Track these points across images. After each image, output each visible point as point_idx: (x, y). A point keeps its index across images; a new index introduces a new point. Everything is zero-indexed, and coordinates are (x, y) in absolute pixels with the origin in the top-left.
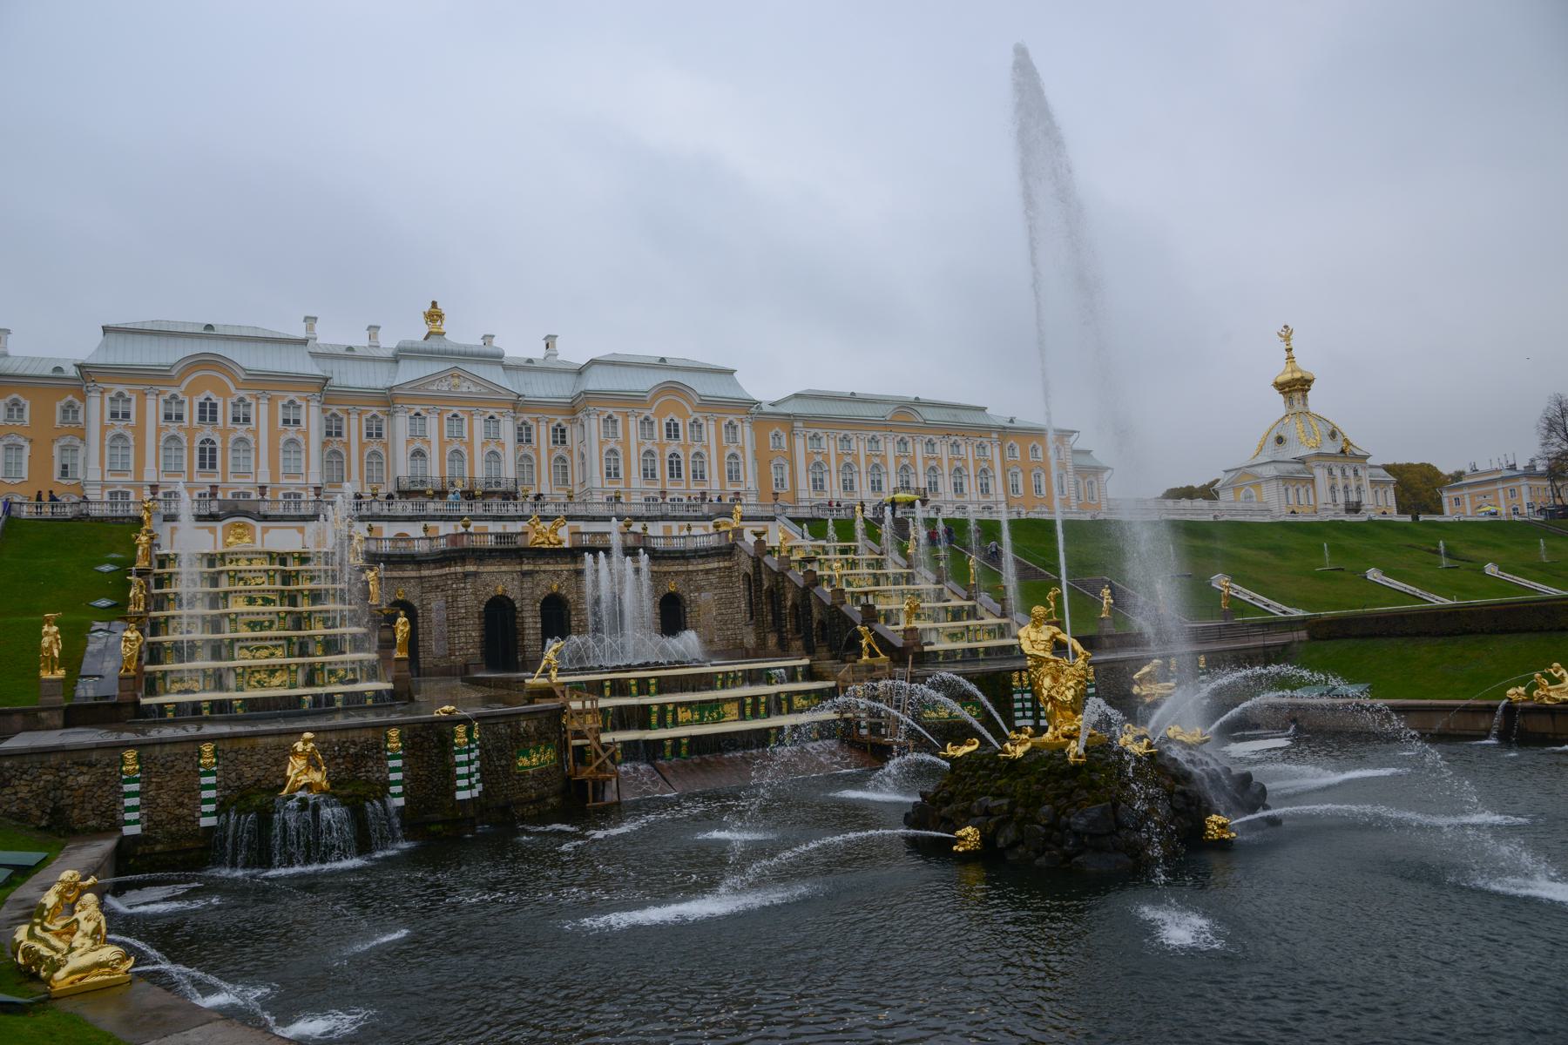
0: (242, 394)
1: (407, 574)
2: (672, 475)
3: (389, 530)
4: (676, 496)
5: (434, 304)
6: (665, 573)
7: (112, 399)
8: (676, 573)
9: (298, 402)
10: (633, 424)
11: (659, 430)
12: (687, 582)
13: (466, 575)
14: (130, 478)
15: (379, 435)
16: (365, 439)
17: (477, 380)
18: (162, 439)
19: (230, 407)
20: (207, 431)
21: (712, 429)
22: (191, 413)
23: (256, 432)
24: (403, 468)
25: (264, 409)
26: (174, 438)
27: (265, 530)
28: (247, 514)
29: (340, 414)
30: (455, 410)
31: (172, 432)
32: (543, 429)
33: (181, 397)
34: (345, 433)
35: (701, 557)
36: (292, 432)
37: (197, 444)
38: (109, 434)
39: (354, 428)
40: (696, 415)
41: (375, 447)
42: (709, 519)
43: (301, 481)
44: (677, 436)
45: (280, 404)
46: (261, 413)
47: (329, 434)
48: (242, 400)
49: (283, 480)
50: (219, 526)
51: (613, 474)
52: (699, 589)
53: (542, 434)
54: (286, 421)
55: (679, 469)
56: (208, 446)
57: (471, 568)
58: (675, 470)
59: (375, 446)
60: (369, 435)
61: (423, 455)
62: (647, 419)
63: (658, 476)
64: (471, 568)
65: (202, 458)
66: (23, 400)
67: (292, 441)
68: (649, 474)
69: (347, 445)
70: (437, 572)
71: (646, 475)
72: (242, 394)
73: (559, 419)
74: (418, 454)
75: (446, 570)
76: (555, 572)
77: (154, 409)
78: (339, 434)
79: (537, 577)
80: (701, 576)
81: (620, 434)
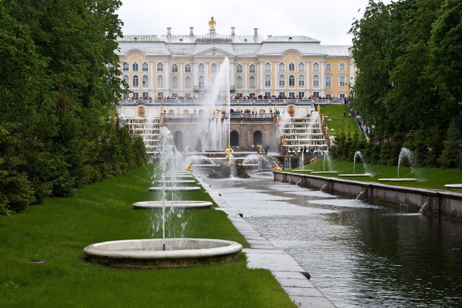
1: (180, 124)
2: (290, 84)
4: (292, 92)
5: (212, 18)
8: (259, 125)
10: (276, 66)
11: (287, 67)
12: (262, 127)
13: (194, 125)
15: (190, 71)
17: (221, 51)
19: (142, 64)
20: (136, 73)
22: (131, 67)
23: (150, 73)
27: (148, 109)
28: (143, 104)
29: (177, 64)
30: (214, 62)
36: (160, 73)
37: (132, 77)
39: (181, 69)
41: (188, 75)
42: (286, 105)
43: (163, 89)
44: (293, 69)
47: (173, 71)
49: (158, 89)
50: (136, 107)
51: (268, 84)
52: (266, 130)
53: (246, 69)
54: (158, 69)
55: (293, 82)
56: (136, 78)
57: (195, 123)
58: (292, 83)
59: (188, 74)
60: (186, 71)
62: (282, 63)
63: (285, 84)
64: (195, 123)
65: (134, 82)
67: (160, 76)
68: (282, 83)
71: (280, 84)
72: (145, 61)
78: (177, 71)
80: (266, 126)
81: (271, 70)
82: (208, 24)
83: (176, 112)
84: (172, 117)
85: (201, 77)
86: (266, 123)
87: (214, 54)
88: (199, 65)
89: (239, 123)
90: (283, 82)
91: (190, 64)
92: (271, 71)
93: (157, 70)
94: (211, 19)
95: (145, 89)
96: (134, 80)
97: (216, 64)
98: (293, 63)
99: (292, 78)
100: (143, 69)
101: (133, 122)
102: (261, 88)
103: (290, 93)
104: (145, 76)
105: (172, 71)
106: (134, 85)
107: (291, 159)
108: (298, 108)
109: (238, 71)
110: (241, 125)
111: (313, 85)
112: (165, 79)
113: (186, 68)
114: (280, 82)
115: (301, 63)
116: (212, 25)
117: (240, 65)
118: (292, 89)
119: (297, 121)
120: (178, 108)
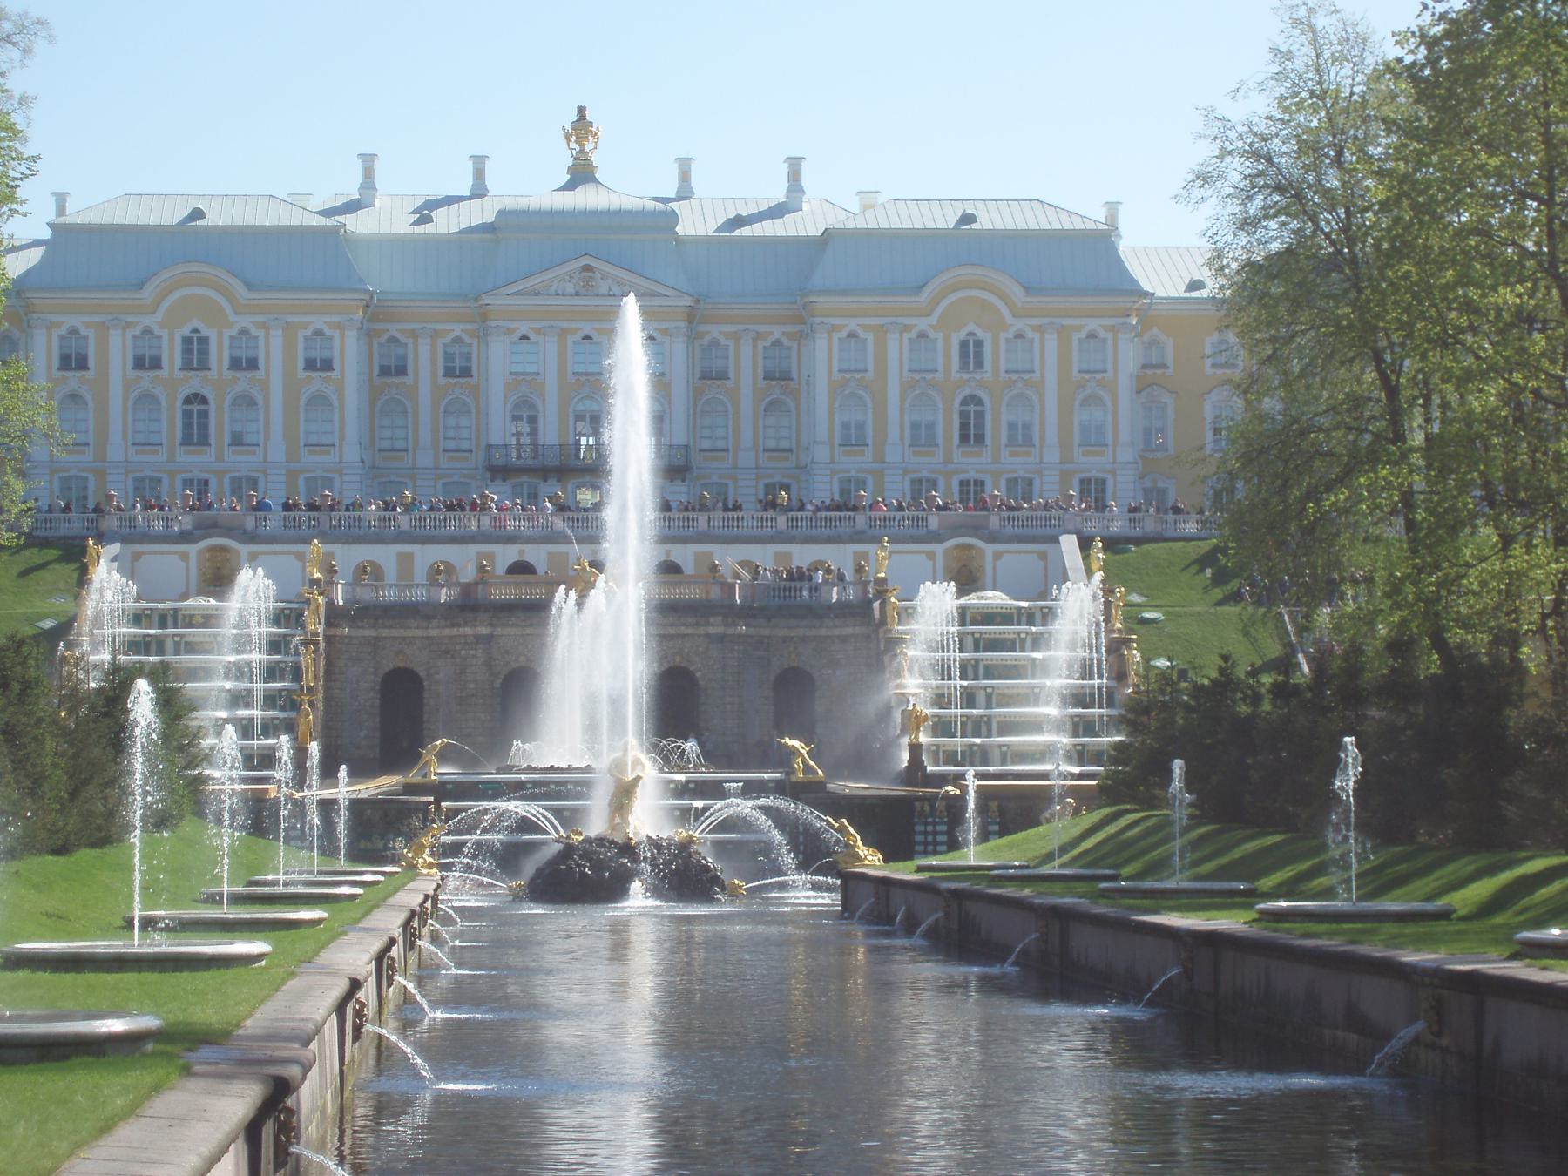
0: (245, 321)
1: (410, 633)
2: (964, 438)
3: (427, 556)
4: (972, 475)
6: (784, 640)
7: (62, 338)
8: (804, 640)
14: (88, 456)
15: (466, 372)
16: (442, 381)
19: (226, 344)
20: (195, 382)
21: (1051, 343)
22: (172, 356)
24: (501, 430)
25: (277, 340)
28: (229, 531)
29: (403, 339)
32: (746, 349)
33: (157, 331)
34: (410, 369)
35: (837, 616)
37: (179, 402)
39: (425, 362)
40: (1020, 324)
44: (979, 364)
46: (272, 351)
48: (244, 332)
50: (193, 550)
51: (853, 438)
53: (746, 364)
54: (310, 365)
56: (195, 407)
58: (971, 433)
60: (449, 372)
61: (532, 406)
62: (922, 335)
63: (940, 441)
65: (187, 426)
68: (922, 436)
70: (447, 632)
72: (245, 321)
73: (777, 332)
75: (455, 631)
77: (118, 351)
78: (401, 371)
81: (871, 367)
83: (391, 575)
84: (368, 595)
86: (837, 632)
88: (512, 343)
89: (702, 631)
90: (931, 427)
91: (468, 340)
92: (870, 375)
93: (301, 364)
95: (242, 462)
96: (187, 415)
98: (980, 334)
99: (972, 408)
100: (236, 364)
101: (170, 621)
102: (822, 454)
103: (962, 483)
105: (376, 371)
106: (187, 441)
108: (997, 556)
109: (706, 375)
110: (707, 635)
111: (1077, 439)
112: (342, 408)
113: (449, 357)
114: (915, 426)
115: (1019, 336)
117: (715, 343)
118: (972, 463)
119: (988, 617)
120: (400, 555)
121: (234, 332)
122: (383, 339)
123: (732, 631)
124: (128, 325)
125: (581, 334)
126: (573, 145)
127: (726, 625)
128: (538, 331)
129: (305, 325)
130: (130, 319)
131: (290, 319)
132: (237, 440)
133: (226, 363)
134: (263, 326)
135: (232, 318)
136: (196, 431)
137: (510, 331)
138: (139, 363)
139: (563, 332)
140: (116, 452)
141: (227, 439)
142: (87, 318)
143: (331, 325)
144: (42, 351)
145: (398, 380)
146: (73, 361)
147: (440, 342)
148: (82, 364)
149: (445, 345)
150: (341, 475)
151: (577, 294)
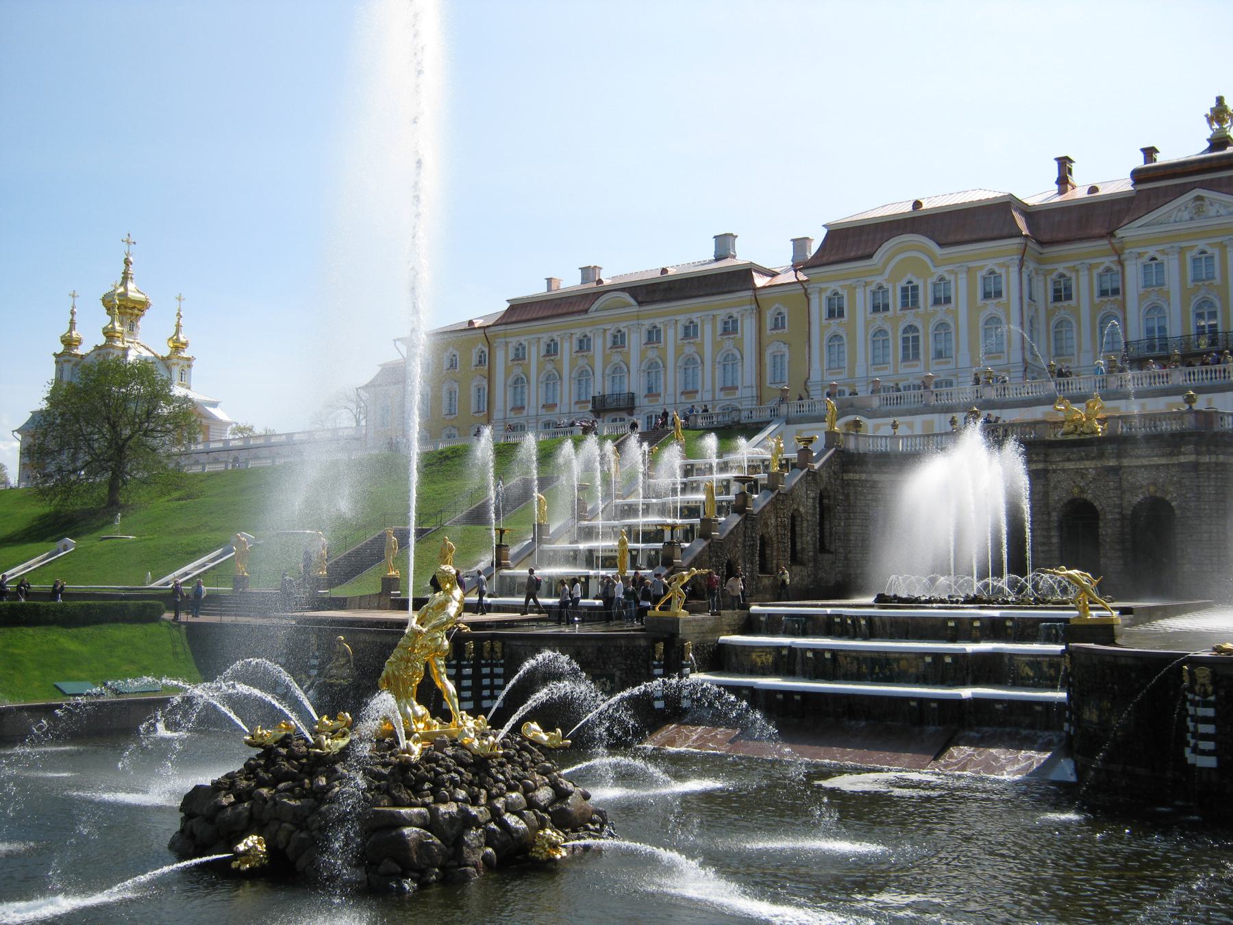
0: (941, 271)
5: (1220, 100)
9: (998, 271)
14: (845, 375)
16: (1097, 300)
18: (871, 332)
20: (910, 318)
22: (895, 299)
26: (881, 332)
29: (1068, 274)
30: (1201, 244)
31: (878, 323)
37: (900, 333)
38: (828, 334)
45: (979, 275)
46: (960, 290)
47: (1057, 298)
48: (942, 279)
54: (987, 295)
56: (910, 335)
61: (1161, 309)
65: (905, 348)
66: (785, 311)
67: (993, 321)
69: (1078, 308)
72: (941, 271)
74: (1154, 309)
76: (1077, 471)
77: (860, 304)
78: (1069, 297)
79: (1054, 479)
82: (1207, 126)
85: (1155, 308)
87: (1199, 211)
89: (1174, 460)
93: (980, 294)
94: (1214, 105)
96: (905, 340)
97: (1209, 251)
100: (937, 301)
104: (943, 325)
105: (1050, 298)
106: (906, 358)
107: (1216, 680)
110: (1180, 464)
116: (1221, 121)
121: (935, 279)
122: (1054, 276)
123: (1206, 459)
124: (866, 284)
125: (1194, 253)
126: (1216, 126)
127: (1198, 453)
128: (1163, 252)
129: (981, 268)
130: (869, 279)
131: (970, 265)
132: (939, 355)
133: (930, 300)
134: (951, 272)
135: (933, 269)
136: (911, 348)
137: (1140, 255)
138: (876, 309)
139: (1182, 251)
140: (860, 371)
141: (932, 354)
142: (841, 283)
143: (1000, 265)
144: (818, 307)
145: (1065, 304)
146: (835, 312)
147: (1095, 272)
148: (841, 314)
149: (1100, 276)
150: (1008, 371)
151: (1192, 219)
